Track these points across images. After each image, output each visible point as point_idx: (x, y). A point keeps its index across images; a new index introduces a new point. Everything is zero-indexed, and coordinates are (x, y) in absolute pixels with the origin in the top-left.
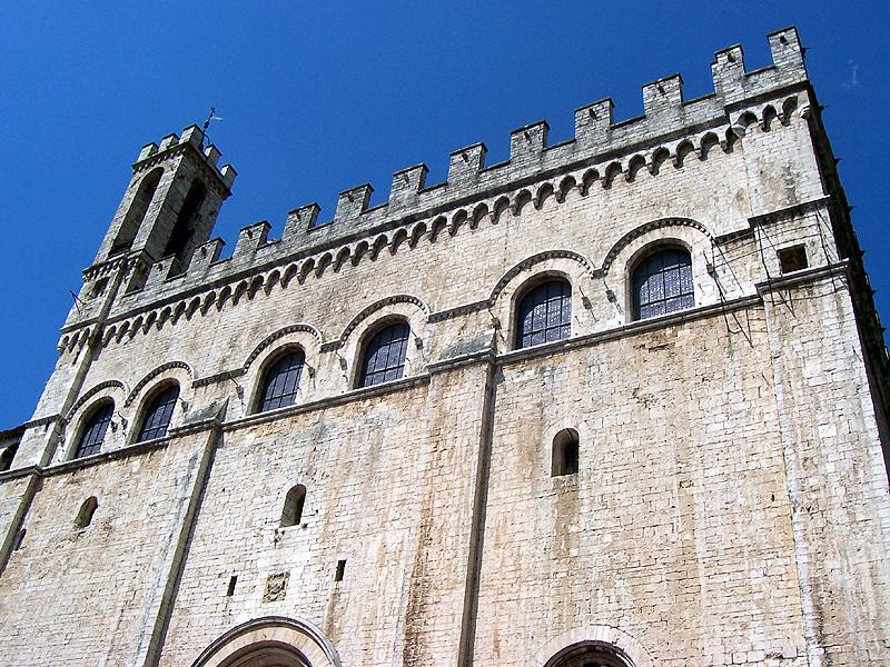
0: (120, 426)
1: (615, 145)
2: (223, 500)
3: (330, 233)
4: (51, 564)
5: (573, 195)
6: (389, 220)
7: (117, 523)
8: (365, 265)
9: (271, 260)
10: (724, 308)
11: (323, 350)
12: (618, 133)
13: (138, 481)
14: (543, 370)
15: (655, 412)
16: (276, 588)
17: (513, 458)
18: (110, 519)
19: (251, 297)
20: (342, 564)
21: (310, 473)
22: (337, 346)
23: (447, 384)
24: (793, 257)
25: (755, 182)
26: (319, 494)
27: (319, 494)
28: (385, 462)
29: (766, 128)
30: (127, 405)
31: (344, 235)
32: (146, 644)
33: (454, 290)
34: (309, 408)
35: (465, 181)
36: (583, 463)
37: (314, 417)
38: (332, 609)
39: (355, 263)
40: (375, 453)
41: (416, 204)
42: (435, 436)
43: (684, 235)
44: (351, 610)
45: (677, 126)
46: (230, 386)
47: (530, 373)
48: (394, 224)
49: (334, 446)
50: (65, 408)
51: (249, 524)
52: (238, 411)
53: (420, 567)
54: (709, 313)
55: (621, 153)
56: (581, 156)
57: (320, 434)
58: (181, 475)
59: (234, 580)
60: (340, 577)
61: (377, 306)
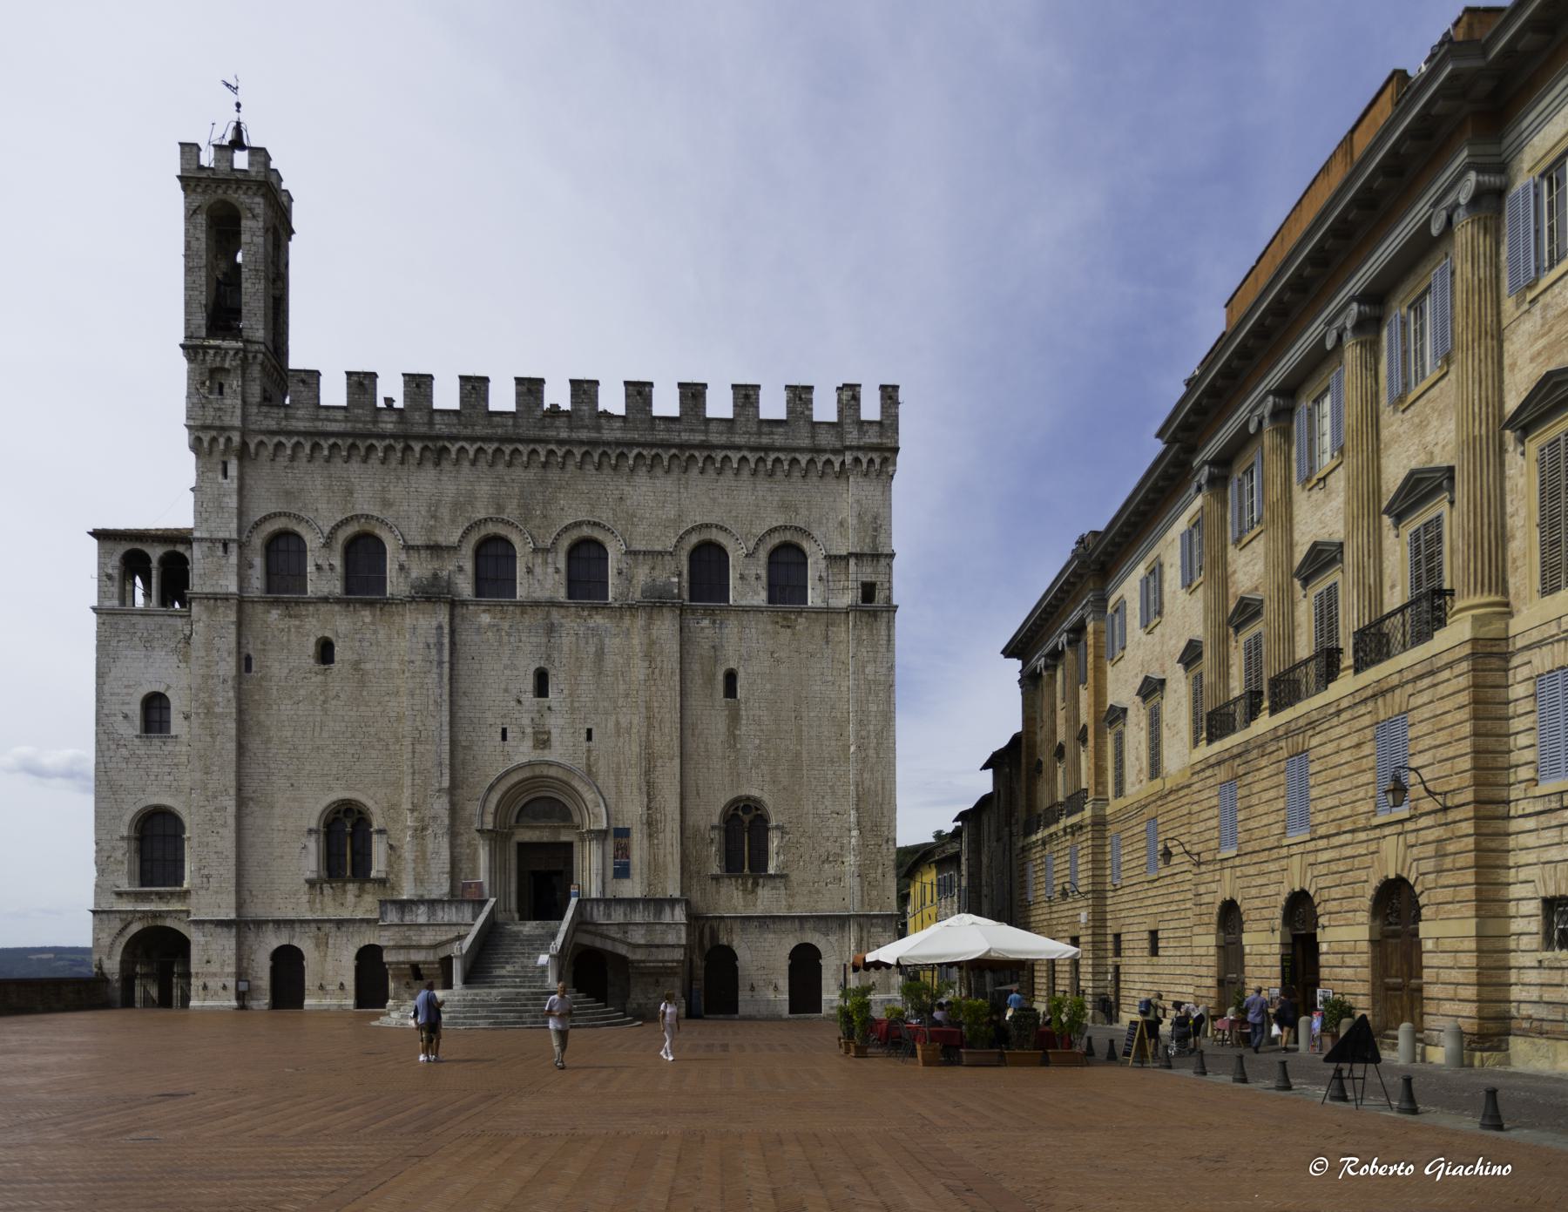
0: (326, 567)
1: (765, 440)
2: (477, 666)
3: (515, 425)
4: (302, 692)
5: (729, 474)
6: (574, 436)
7: (368, 666)
8: (553, 475)
9: (454, 431)
10: (828, 611)
11: (536, 551)
12: (765, 429)
13: (375, 632)
14: (714, 622)
15: (783, 669)
16: (542, 741)
17: (699, 681)
18: (358, 663)
19: (437, 464)
20: (589, 732)
21: (549, 657)
22: (547, 551)
23: (651, 618)
24: (868, 591)
25: (852, 521)
26: (562, 676)
27: (562, 676)
28: (609, 664)
29: (866, 475)
30: (327, 545)
31: (532, 433)
32: (446, 771)
33: (640, 529)
34: (536, 604)
35: (643, 422)
36: (741, 693)
37: (540, 613)
38: (588, 758)
39: (545, 465)
40: (600, 654)
41: (598, 429)
42: (649, 657)
43: (807, 546)
44: (601, 762)
45: (806, 443)
46: (448, 567)
47: (706, 623)
48: (581, 443)
49: (566, 641)
50: (240, 531)
51: (506, 690)
52: (465, 586)
53: (648, 745)
54: (818, 611)
55: (767, 449)
56: (738, 440)
57: (551, 629)
58: (432, 641)
59: (504, 731)
60: (589, 738)
61: (578, 524)
